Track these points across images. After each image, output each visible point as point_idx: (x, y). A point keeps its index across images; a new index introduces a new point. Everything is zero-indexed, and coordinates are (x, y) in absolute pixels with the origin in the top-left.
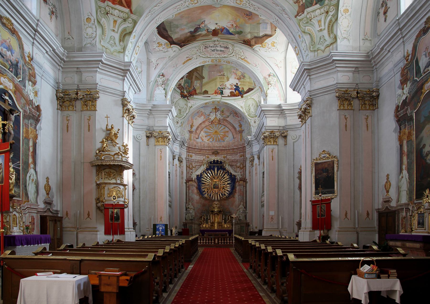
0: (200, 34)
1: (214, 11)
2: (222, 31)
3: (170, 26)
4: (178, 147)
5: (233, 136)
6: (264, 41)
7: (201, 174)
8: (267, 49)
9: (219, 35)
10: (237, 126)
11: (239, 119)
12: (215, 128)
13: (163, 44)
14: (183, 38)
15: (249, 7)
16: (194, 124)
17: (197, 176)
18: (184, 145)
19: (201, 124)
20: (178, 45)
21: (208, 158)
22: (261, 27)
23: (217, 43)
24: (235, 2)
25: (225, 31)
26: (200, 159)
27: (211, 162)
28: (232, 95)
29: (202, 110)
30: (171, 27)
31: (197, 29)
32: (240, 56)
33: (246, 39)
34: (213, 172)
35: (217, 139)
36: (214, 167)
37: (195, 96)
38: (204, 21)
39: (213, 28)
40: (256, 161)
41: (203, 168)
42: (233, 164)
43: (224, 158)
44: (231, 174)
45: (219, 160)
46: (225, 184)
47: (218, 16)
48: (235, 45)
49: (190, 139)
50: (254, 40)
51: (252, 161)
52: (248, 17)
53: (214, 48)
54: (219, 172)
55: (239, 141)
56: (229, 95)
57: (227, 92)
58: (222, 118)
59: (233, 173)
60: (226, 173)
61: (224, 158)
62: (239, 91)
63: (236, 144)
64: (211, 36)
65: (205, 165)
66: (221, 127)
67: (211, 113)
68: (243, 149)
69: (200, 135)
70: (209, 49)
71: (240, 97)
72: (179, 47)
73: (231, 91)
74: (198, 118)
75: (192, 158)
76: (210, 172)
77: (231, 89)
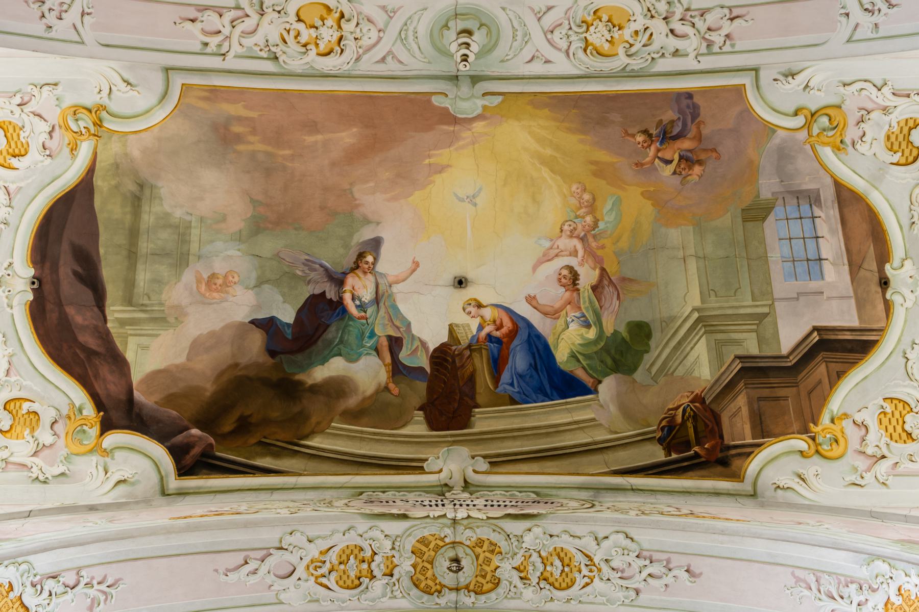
0: (337, 389)
1: (442, 156)
2: (497, 365)
3: (134, 234)
6: (824, 400)
8: (861, 463)
9: (485, 420)
13: (48, 415)
14: (205, 373)
15: (673, 43)
20: (161, 438)
22: (777, 253)
24: (577, 45)
25: (519, 361)
30: (132, 256)
31: (321, 320)
38: (376, 244)
39: (435, 337)
47: (472, 199)
50: (741, 402)
52: (672, 152)
64: (418, 427)
72: (167, 462)
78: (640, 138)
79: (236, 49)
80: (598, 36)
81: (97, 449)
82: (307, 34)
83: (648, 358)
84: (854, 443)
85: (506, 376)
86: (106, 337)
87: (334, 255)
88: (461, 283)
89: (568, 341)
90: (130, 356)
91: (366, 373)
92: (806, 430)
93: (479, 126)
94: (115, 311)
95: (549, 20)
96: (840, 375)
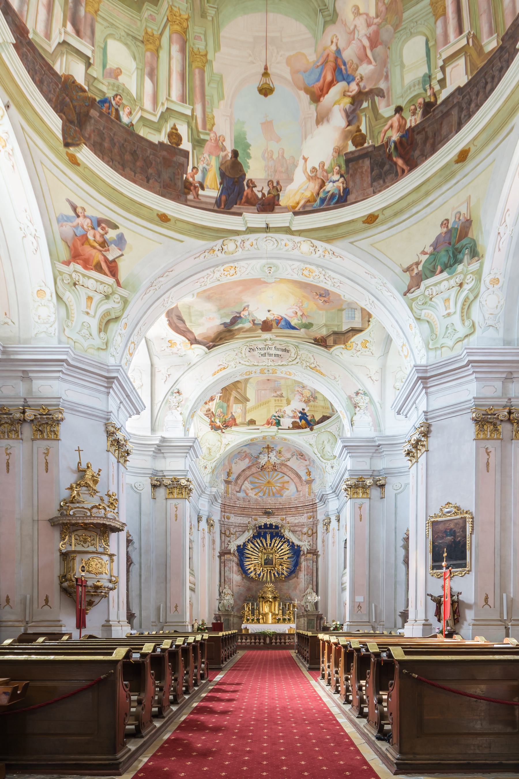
0: (240, 330)
2: (278, 324)
4: (206, 504)
5: (297, 488)
6: (350, 339)
7: (245, 545)
8: (355, 351)
9: (274, 331)
10: (303, 473)
11: (307, 463)
12: (267, 477)
16: (233, 470)
17: (239, 547)
18: (216, 501)
19: (244, 471)
20: (204, 345)
21: (256, 520)
23: (269, 343)
24: (300, 273)
25: (283, 323)
26: (242, 522)
27: (260, 527)
28: (296, 426)
29: (245, 449)
31: (236, 320)
32: (308, 364)
33: (318, 336)
34: (264, 541)
35: (271, 493)
36: (265, 533)
37: (234, 428)
38: (248, 306)
40: (334, 523)
41: (248, 535)
42: (296, 529)
43: (282, 520)
44: (293, 543)
45: (274, 524)
46: (283, 558)
48: (301, 346)
49: (226, 492)
50: (332, 338)
51: (327, 524)
53: (265, 351)
54: (273, 541)
55: (307, 495)
56: (291, 426)
57: (287, 422)
58: (278, 462)
59: (297, 542)
60: (285, 542)
61: (282, 520)
62: (306, 420)
63: (302, 499)
64: (260, 331)
65: (251, 531)
66: (278, 475)
67: (260, 453)
68: (312, 507)
69: (243, 487)
70: (256, 353)
71: (308, 429)
72: (206, 349)
73: (293, 420)
74: (240, 462)
75: (230, 521)
76: (259, 541)
77: (294, 417)
78: (315, 294)
79: (209, 282)
80: (306, 273)
81: (191, 348)
82: (226, 273)
83: (312, 328)
84: (354, 347)
85: (280, 325)
86: (187, 328)
87: (238, 309)
88: (269, 311)
89: (294, 322)
90: (193, 331)
91: (248, 325)
92: (345, 344)
93: (273, 284)
94: (188, 325)
95: (293, 267)
96: (354, 335)
